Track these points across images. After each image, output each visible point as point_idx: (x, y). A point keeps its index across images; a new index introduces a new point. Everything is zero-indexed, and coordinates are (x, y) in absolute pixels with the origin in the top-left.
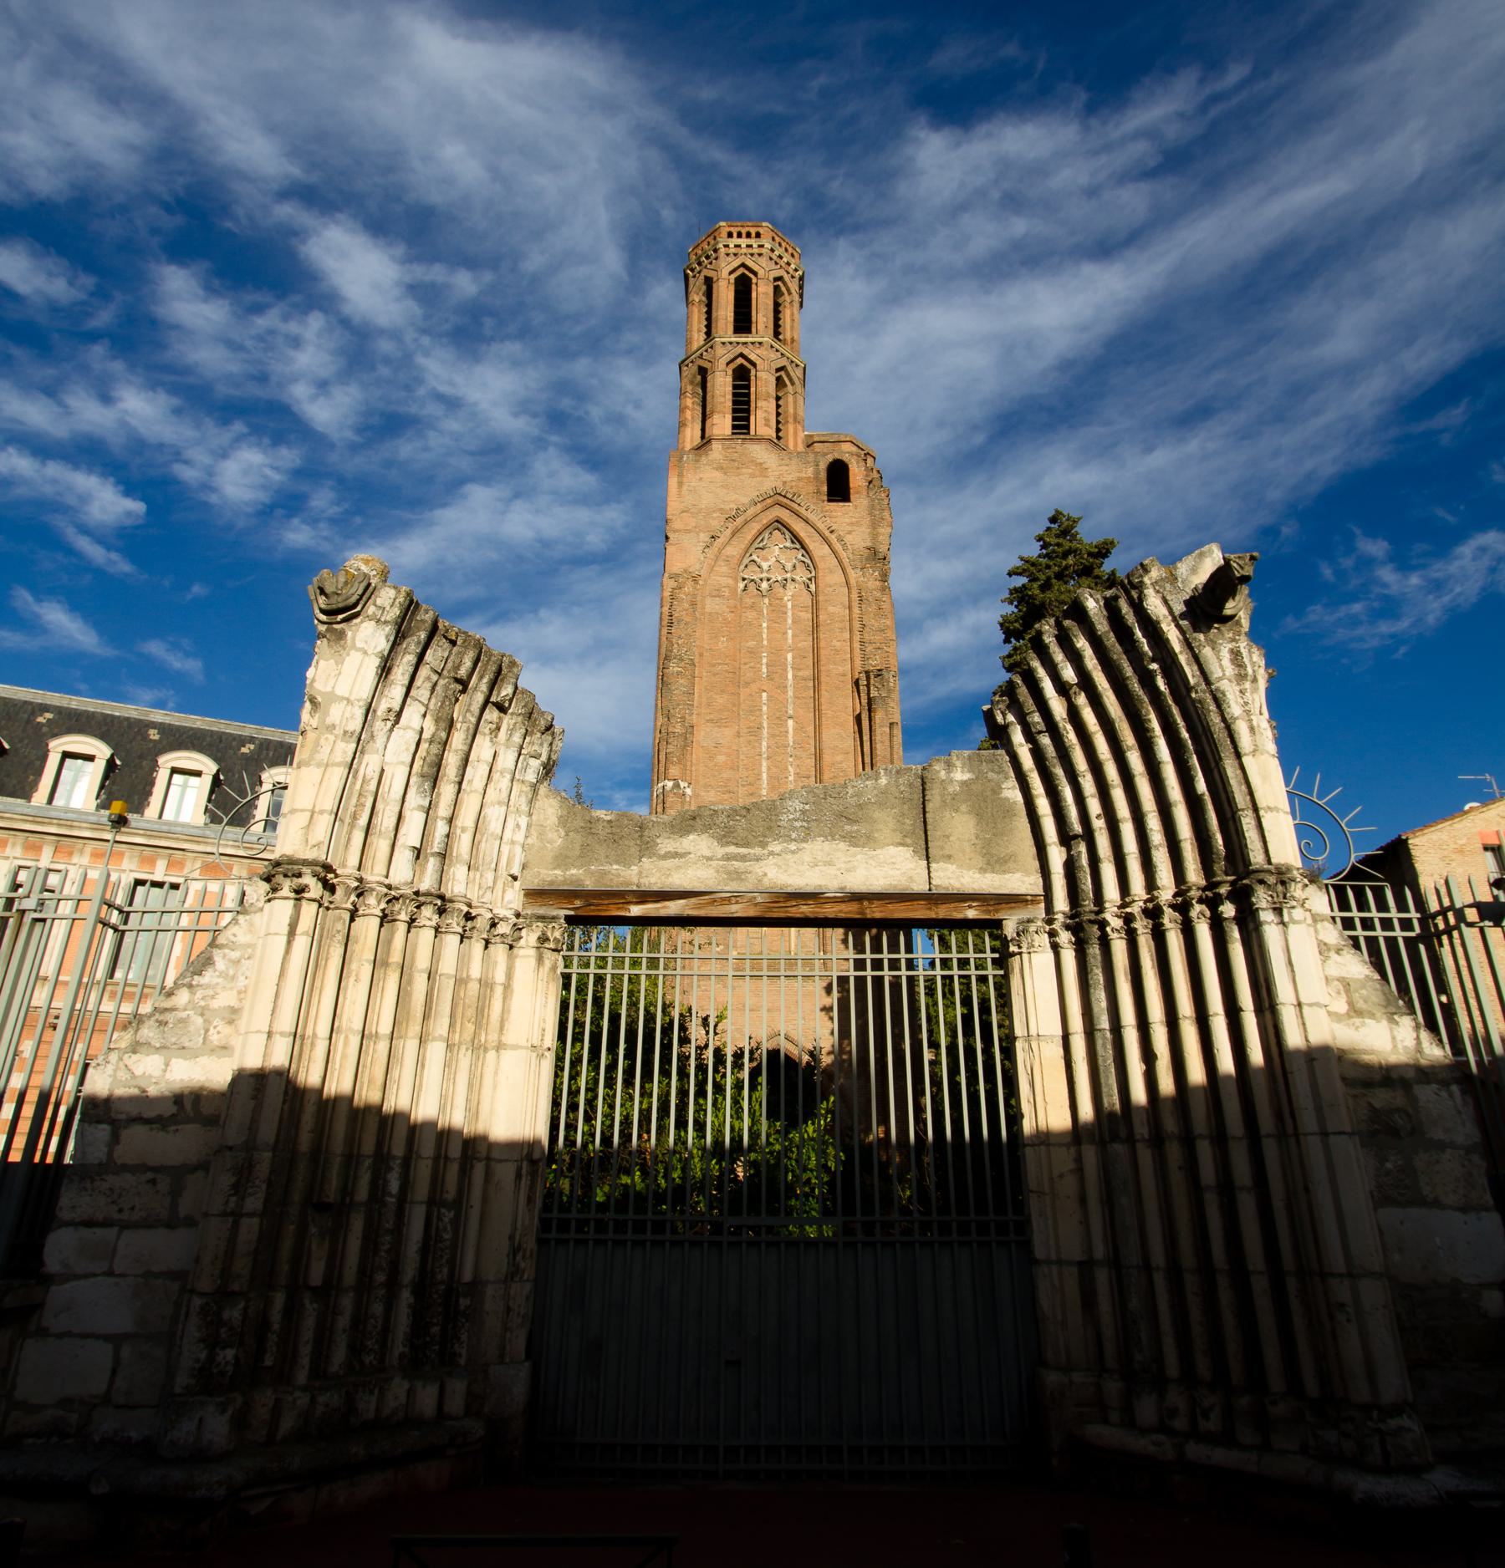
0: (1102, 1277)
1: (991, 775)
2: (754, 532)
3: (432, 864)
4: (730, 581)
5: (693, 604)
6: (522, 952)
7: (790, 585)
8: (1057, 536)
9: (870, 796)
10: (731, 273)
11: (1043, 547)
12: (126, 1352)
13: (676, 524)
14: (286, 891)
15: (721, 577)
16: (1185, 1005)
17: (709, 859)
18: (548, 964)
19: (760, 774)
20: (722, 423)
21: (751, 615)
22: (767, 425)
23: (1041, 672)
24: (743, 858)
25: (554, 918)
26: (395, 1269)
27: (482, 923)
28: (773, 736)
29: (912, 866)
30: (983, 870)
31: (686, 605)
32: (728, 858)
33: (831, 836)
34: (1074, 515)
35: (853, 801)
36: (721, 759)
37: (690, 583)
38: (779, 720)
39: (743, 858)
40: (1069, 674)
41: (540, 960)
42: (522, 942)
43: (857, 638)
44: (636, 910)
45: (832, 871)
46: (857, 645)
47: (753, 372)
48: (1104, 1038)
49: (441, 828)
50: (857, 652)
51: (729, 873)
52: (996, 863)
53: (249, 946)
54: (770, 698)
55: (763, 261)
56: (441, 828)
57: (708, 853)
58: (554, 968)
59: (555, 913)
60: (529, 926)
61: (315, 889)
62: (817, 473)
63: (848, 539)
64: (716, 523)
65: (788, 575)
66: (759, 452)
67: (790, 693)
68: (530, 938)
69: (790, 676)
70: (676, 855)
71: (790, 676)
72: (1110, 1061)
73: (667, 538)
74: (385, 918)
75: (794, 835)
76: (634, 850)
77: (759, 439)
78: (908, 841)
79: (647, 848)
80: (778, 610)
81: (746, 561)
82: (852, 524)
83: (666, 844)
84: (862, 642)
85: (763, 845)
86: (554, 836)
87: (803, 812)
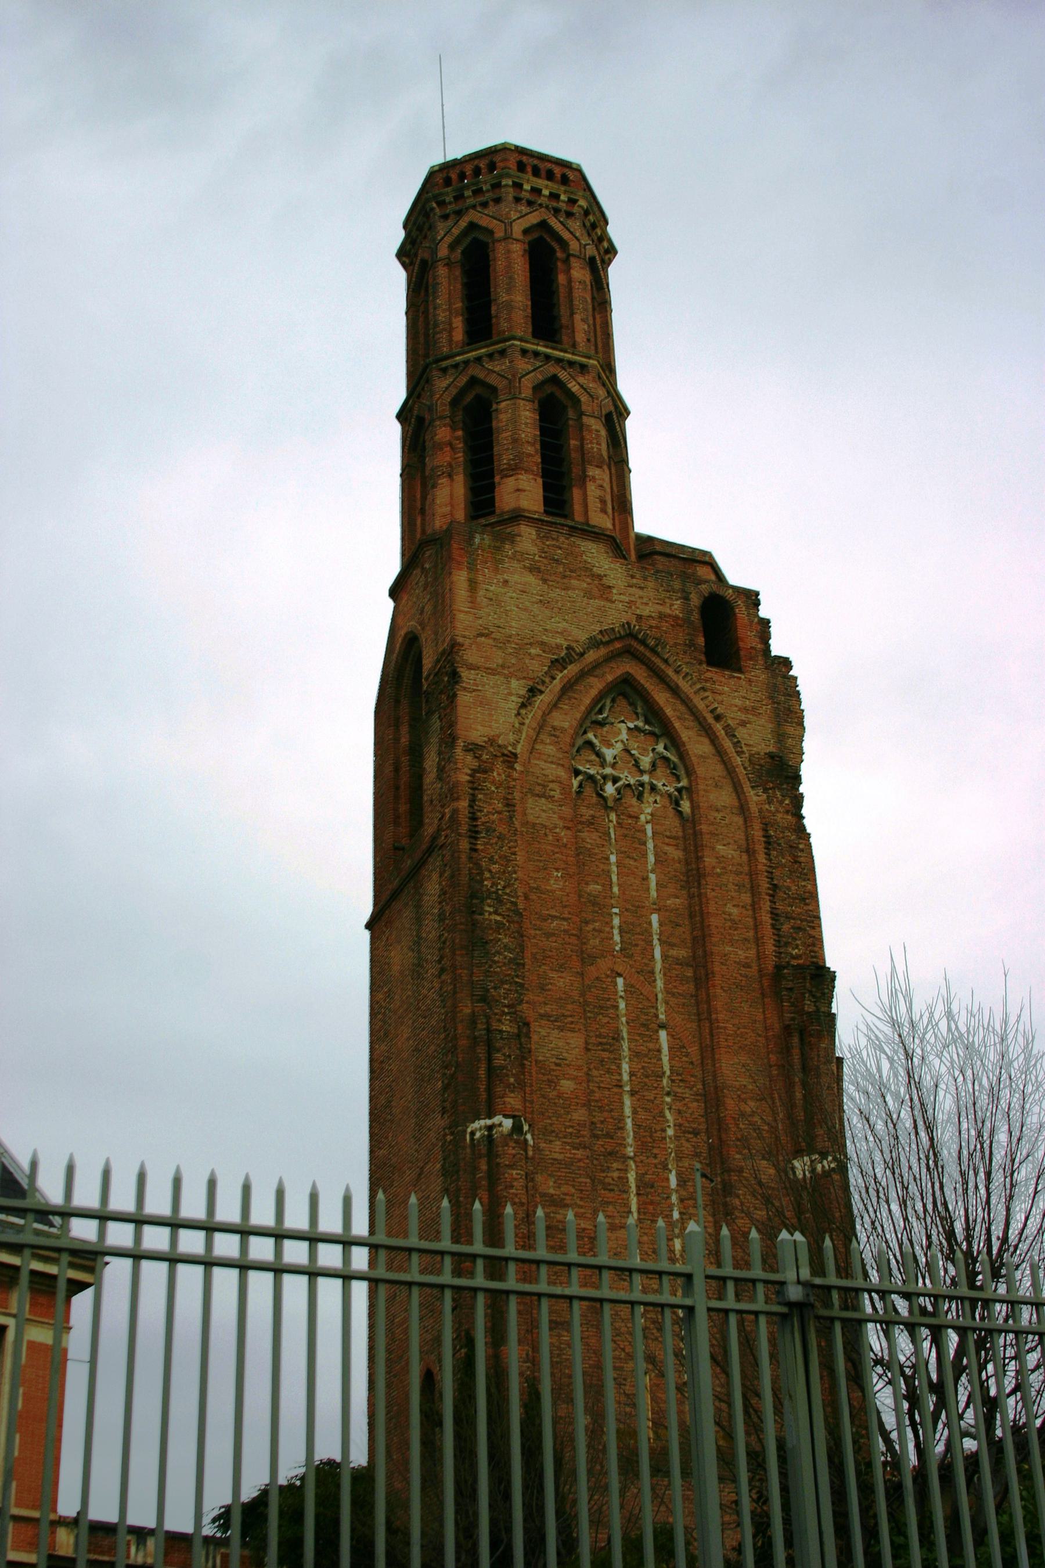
2: (594, 692)
4: (562, 773)
5: (509, 804)
10: (526, 232)
13: (471, 656)
19: (621, 1119)
20: (522, 491)
21: (590, 838)
22: (604, 511)
28: (636, 1055)
31: (500, 806)
36: (567, 1085)
38: (645, 1026)
43: (766, 906)
46: (766, 918)
47: (571, 414)
50: (768, 931)
54: (629, 988)
55: (575, 225)
63: (741, 733)
64: (537, 667)
65: (646, 778)
67: (660, 984)
80: (632, 836)
81: (580, 742)
82: (745, 710)
84: (774, 915)
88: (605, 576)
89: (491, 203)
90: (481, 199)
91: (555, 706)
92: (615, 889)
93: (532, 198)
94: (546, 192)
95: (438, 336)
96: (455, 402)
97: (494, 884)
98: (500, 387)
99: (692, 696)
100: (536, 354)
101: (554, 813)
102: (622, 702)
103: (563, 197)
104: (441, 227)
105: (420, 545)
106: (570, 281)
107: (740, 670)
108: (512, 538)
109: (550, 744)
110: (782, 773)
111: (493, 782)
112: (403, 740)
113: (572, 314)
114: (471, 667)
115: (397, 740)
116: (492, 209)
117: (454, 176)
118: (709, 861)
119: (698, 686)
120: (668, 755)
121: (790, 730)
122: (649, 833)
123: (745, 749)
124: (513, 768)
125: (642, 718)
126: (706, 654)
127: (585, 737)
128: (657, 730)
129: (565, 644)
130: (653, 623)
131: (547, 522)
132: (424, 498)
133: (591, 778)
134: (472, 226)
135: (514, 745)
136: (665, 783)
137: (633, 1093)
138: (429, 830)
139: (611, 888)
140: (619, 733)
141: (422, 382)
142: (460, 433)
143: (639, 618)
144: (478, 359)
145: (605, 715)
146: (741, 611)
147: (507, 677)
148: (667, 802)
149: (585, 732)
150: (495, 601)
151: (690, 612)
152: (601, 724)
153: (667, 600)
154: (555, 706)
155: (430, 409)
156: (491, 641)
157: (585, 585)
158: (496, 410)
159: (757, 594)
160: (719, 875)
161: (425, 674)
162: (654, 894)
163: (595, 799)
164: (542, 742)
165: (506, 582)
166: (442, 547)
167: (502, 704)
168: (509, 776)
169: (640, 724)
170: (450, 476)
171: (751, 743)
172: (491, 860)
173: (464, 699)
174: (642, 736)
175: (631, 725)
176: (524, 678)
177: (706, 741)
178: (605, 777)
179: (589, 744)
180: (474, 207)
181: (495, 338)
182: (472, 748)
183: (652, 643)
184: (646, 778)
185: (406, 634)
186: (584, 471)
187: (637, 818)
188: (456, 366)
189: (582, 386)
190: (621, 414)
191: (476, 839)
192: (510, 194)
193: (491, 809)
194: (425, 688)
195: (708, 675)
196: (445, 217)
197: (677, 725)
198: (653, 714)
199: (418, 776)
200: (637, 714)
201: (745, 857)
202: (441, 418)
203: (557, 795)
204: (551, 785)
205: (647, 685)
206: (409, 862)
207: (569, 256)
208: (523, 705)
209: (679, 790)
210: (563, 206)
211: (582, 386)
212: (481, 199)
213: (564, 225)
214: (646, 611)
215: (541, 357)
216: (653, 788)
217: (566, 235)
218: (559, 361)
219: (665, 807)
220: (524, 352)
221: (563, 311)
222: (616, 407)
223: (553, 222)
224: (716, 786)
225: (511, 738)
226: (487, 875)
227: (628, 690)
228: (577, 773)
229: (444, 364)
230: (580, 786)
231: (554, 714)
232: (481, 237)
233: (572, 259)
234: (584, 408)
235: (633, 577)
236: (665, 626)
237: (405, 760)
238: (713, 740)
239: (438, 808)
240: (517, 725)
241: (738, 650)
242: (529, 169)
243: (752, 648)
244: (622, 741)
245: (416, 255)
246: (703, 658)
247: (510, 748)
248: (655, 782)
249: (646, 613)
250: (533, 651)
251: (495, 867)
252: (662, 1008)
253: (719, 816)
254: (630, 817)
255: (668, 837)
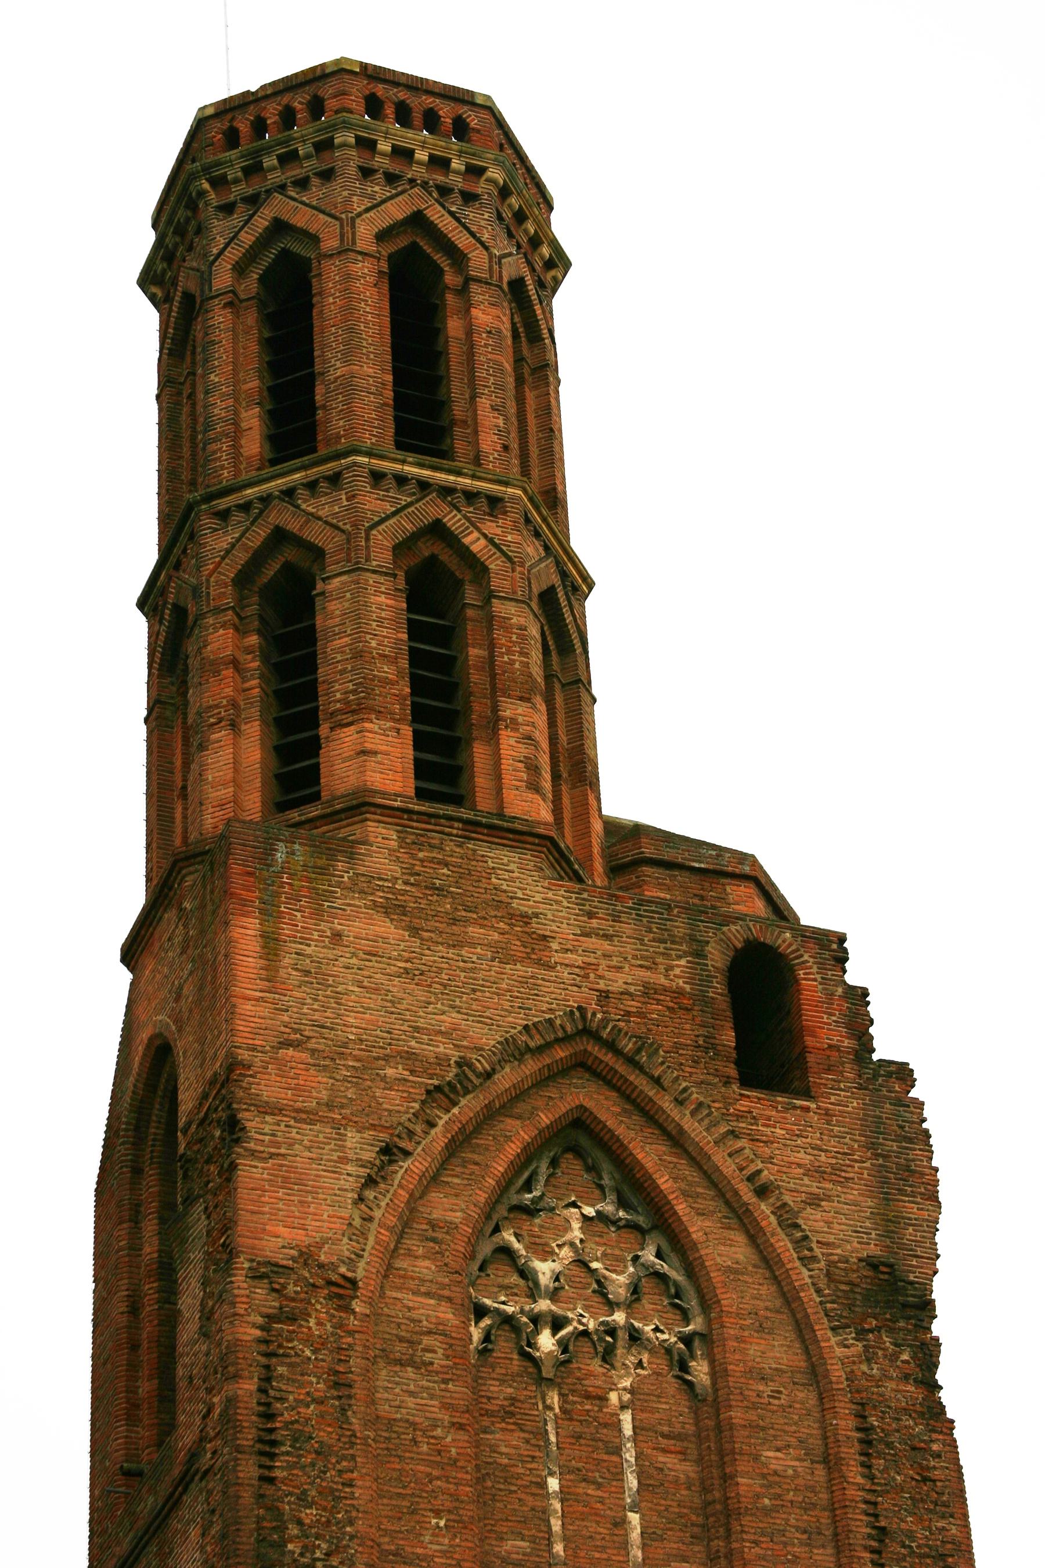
2: (513, 1149)
4: (448, 1315)
5: (340, 1383)
10: (382, 236)
13: (268, 1087)
20: (373, 754)
21: (507, 1443)
22: (534, 787)
47: (471, 595)
55: (481, 219)
62: (699, 976)
63: (812, 1220)
64: (397, 1103)
65: (619, 1317)
80: (592, 1434)
81: (486, 1249)
82: (816, 1172)
88: (536, 915)
89: (315, 181)
90: (296, 172)
91: (433, 1180)
92: (559, 1548)
93: (395, 168)
94: (422, 155)
95: (214, 447)
96: (243, 579)
97: (306, 1549)
98: (329, 548)
99: (710, 1149)
100: (401, 480)
101: (432, 1397)
102: (571, 1164)
103: (456, 164)
104: (219, 229)
105: (174, 864)
106: (469, 332)
107: (807, 1094)
108: (350, 850)
109: (425, 1257)
110: (896, 1299)
111: (307, 1341)
112: (147, 1249)
113: (473, 397)
115: (135, 1248)
116: (316, 192)
117: (244, 127)
118: (746, 1483)
119: (723, 1129)
120: (664, 1267)
121: (912, 1209)
122: (628, 1429)
123: (818, 1251)
124: (348, 1309)
125: (612, 1197)
126: (738, 1063)
127: (496, 1239)
128: (641, 1220)
129: (455, 1055)
130: (632, 1005)
131: (419, 813)
132: (186, 765)
133: (508, 1320)
134: (279, 227)
135: (351, 1264)
136: (658, 1328)
138: (186, 1438)
139: (550, 1545)
140: (568, 1228)
141: (183, 538)
142: (254, 639)
143: (604, 996)
144: (289, 493)
145: (537, 1193)
146: (809, 978)
147: (336, 1125)
148: (662, 1364)
149: (497, 1230)
150: (314, 975)
151: (706, 981)
152: (530, 1211)
153: (660, 960)
154: (433, 1180)
155: (196, 591)
156: (304, 1056)
157: (496, 936)
158: (323, 593)
159: (842, 938)
160: (767, 1512)
161: (182, 1122)
162: (637, 1553)
163: (516, 1363)
164: (410, 1254)
165: (337, 936)
166: (212, 869)
167: (328, 1181)
168: (340, 1326)
169: (609, 1208)
170: (234, 725)
171: (831, 1239)
172: (303, 1499)
173: (251, 1173)
174: (612, 1233)
175: (589, 1211)
176: (373, 1127)
177: (740, 1238)
178: (536, 1320)
179: (506, 1252)
180: (282, 188)
181: (323, 451)
182: (268, 1273)
183: (628, 1046)
184: (619, 1317)
185: (151, 1039)
186: (495, 709)
187: (604, 1399)
188: (246, 507)
189: (491, 541)
190: (575, 589)
191: (272, 1456)
192: (350, 161)
193: (303, 1396)
194: (181, 1149)
195: (743, 1105)
196: (228, 209)
197: (681, 1208)
198: (633, 1186)
199: (170, 1320)
200: (601, 1188)
201: (821, 1472)
202: (218, 611)
203: (438, 1359)
204: (427, 1341)
205: (620, 1131)
206: (151, 1499)
207: (468, 280)
208: (370, 1182)
209: (687, 1340)
210: (456, 181)
211: (491, 541)
212: (296, 172)
213: (458, 220)
214: (617, 982)
215: (412, 487)
216: (635, 1337)
217: (462, 240)
218: (447, 491)
219: (658, 1374)
220: (377, 477)
221: (457, 390)
222: (564, 575)
223: (437, 215)
224: (761, 1328)
225: (345, 1247)
226: (294, 1530)
227: (584, 1141)
228: (480, 1312)
229: (223, 503)
230: (487, 1338)
231: (434, 1196)
232: (296, 248)
233: (474, 287)
234: (495, 583)
235: (591, 915)
236: (655, 1011)
237: (150, 1288)
238: (755, 1236)
239: (202, 1394)
240: (357, 1222)
241: (804, 1050)
242: (389, 111)
243: (830, 1046)
244: (572, 1244)
245: (174, 282)
246: (732, 1071)
247: (343, 1270)
248: (636, 1324)
249: (618, 986)
250: (390, 1072)
251: (309, 1515)
253: (766, 1389)
254: (588, 1396)
255: (664, 1436)
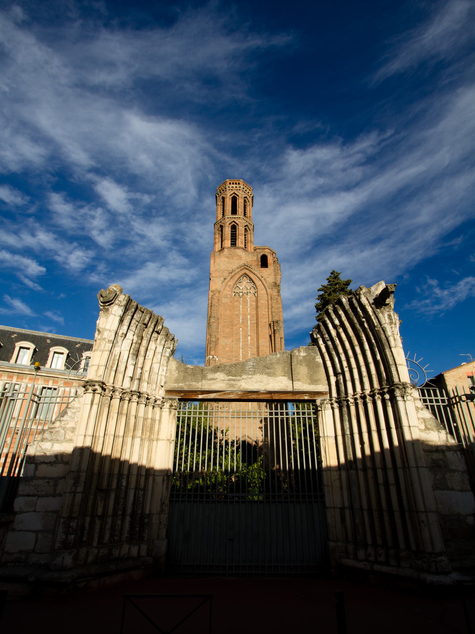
0: (347, 512)
1: (312, 354)
2: (238, 277)
3: (136, 382)
4: (230, 293)
5: (219, 300)
6: (164, 410)
7: (249, 294)
8: (333, 279)
9: (274, 361)
11: (328, 282)
12: (40, 536)
13: (213, 275)
14: (90, 391)
15: (227, 292)
16: (373, 427)
17: (223, 380)
18: (173, 413)
19: (239, 354)
20: (228, 243)
21: (237, 303)
23: (328, 322)
24: (234, 380)
25: (175, 399)
26: (124, 509)
27: (152, 401)
28: (243, 342)
29: (288, 382)
30: (310, 384)
31: (216, 300)
32: (229, 380)
33: (262, 373)
34: (339, 272)
35: (269, 362)
36: (227, 349)
37: (217, 293)
38: (245, 336)
39: (234, 380)
40: (337, 322)
41: (170, 412)
42: (165, 407)
43: (270, 311)
44: (200, 397)
45: (262, 384)
46: (270, 313)
47: (237, 227)
48: (348, 437)
49: (139, 371)
51: (230, 385)
52: (314, 381)
53: (79, 408)
54: (243, 330)
56: (139, 371)
57: (223, 379)
58: (175, 415)
59: (175, 397)
60: (167, 401)
61: (99, 390)
62: (257, 259)
63: (267, 279)
64: (226, 274)
65: (248, 291)
66: (239, 252)
67: (249, 328)
68: (167, 405)
69: (249, 323)
70: (213, 379)
71: (249, 323)
72: (350, 444)
73: (210, 279)
74: (121, 399)
75: (250, 373)
76: (200, 378)
77: (239, 248)
78: (286, 375)
79: (204, 377)
80: (245, 302)
81: (235, 286)
83: (210, 376)
84: (272, 312)
85: (241, 376)
86: (175, 373)
87: (253, 366)
107: (267, 267)
114: (213, 277)
137: (242, 349)
150: (218, 264)
214: (249, 260)
218: (235, 218)
252: (249, 332)
